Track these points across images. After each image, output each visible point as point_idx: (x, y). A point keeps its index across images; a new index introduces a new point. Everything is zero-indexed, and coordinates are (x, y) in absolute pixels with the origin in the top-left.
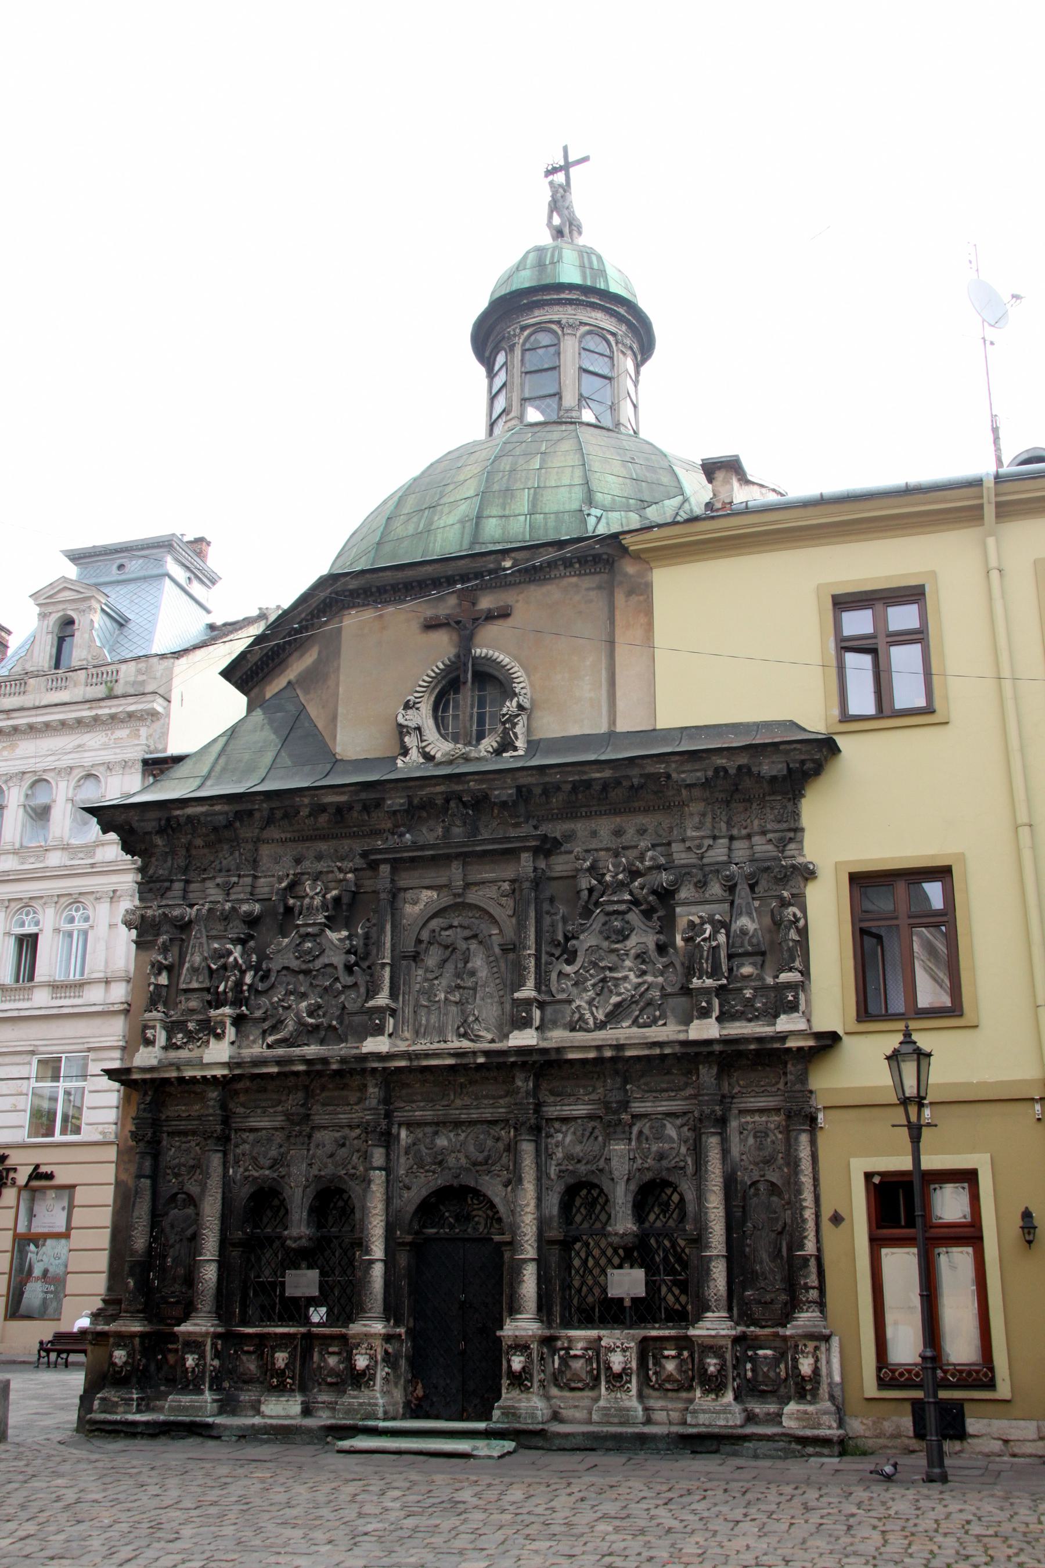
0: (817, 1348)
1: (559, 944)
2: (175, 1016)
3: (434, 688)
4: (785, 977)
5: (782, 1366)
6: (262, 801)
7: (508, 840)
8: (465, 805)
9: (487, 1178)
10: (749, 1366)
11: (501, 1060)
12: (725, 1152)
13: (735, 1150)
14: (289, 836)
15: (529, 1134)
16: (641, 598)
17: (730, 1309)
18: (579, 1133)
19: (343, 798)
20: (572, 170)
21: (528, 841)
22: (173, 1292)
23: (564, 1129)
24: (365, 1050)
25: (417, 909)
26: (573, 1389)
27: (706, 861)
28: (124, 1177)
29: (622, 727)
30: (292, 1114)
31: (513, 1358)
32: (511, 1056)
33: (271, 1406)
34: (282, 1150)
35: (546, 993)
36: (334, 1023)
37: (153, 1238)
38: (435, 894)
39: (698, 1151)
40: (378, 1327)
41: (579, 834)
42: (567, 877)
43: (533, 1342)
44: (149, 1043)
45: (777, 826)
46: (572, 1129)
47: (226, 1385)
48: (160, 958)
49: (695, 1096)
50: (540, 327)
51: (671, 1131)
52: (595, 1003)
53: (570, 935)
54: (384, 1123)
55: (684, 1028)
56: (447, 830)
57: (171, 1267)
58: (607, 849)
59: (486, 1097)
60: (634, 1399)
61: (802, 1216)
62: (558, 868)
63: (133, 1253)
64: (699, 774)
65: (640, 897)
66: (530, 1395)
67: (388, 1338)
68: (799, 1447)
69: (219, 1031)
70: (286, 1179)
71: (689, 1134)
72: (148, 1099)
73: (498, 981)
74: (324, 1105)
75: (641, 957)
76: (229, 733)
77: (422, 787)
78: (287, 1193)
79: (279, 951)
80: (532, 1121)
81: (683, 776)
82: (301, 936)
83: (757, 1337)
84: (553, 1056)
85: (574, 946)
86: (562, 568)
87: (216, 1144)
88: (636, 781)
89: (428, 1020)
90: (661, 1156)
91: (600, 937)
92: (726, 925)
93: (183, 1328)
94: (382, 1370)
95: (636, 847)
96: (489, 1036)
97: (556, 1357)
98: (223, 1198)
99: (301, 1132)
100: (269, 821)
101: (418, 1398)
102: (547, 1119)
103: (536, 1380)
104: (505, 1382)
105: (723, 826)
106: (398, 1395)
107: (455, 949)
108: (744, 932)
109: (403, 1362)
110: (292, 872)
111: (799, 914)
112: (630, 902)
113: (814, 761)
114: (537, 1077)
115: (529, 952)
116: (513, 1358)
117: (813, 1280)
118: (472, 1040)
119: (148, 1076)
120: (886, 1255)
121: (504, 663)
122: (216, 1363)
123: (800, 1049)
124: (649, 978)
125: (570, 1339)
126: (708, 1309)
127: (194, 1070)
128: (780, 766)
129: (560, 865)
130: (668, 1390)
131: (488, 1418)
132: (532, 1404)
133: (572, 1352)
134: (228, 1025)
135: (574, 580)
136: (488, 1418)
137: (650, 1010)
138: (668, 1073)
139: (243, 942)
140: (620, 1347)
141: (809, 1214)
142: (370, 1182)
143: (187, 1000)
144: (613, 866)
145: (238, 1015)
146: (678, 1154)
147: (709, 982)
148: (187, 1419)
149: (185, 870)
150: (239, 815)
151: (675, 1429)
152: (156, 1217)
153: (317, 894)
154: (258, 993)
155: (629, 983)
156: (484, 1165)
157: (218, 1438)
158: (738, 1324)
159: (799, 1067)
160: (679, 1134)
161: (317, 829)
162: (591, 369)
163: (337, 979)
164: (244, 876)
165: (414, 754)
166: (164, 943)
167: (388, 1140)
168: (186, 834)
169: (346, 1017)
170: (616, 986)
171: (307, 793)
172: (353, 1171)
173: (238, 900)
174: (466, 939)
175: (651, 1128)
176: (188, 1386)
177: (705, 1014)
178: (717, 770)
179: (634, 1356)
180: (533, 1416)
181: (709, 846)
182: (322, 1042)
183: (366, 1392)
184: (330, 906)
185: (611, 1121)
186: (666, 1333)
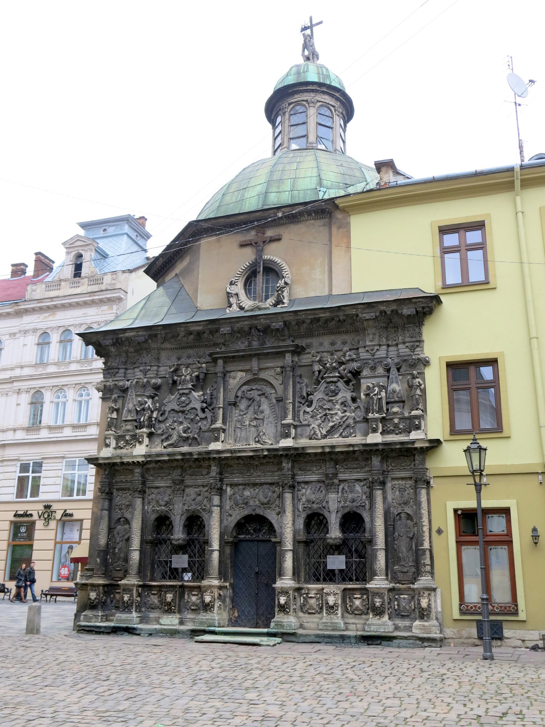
1: (304, 398)
2: (120, 433)
3: (244, 275)
4: (414, 413)
5: (412, 603)
6: (162, 330)
7: (280, 347)
8: (259, 331)
10: (396, 603)
11: (275, 453)
12: (385, 498)
13: (390, 498)
14: (174, 346)
16: (345, 230)
17: (387, 575)
18: (313, 489)
19: (200, 328)
20: (314, 28)
21: (289, 347)
23: (306, 487)
24: (210, 449)
25: (235, 381)
26: (310, 613)
27: (375, 357)
28: (96, 510)
29: (334, 293)
30: (176, 480)
31: (281, 598)
32: (280, 451)
33: (164, 620)
34: (170, 497)
35: (297, 421)
36: (196, 436)
37: (109, 539)
38: (244, 374)
39: (371, 497)
40: (216, 582)
41: (314, 344)
42: (308, 365)
44: (107, 446)
47: (143, 609)
48: (113, 405)
49: (370, 471)
50: (298, 103)
51: (358, 488)
52: (321, 426)
53: (309, 393)
54: (219, 484)
55: (365, 438)
56: (250, 344)
57: (118, 553)
58: (328, 352)
59: (269, 471)
60: (340, 618)
61: (422, 530)
62: (304, 361)
63: (99, 546)
64: (372, 314)
65: (344, 374)
67: (220, 588)
68: (420, 643)
69: (140, 440)
72: (107, 472)
73: (274, 416)
74: (191, 475)
75: (343, 404)
76: (147, 298)
77: (238, 322)
78: (173, 518)
79: (170, 402)
80: (291, 483)
81: (364, 315)
82: (180, 395)
83: (399, 589)
84: (300, 451)
85: (311, 398)
86: (306, 216)
87: (139, 494)
88: (341, 318)
89: (241, 434)
90: (353, 501)
91: (324, 394)
92: (385, 388)
93: (123, 582)
95: (341, 350)
96: (270, 442)
97: (302, 598)
98: (142, 520)
100: (165, 340)
101: (235, 617)
102: (298, 482)
103: (292, 609)
104: (277, 609)
105: (384, 340)
106: (225, 616)
107: (254, 400)
108: (394, 391)
109: (228, 600)
110: (176, 363)
111: (421, 382)
112: (339, 377)
113: (428, 307)
114: (293, 462)
116: (281, 598)
117: (428, 561)
118: (262, 444)
119: (107, 461)
120: (464, 549)
121: (278, 262)
122: (139, 599)
123: (422, 448)
124: (348, 414)
125: (308, 589)
128: (412, 310)
129: (305, 359)
130: (356, 614)
131: (267, 626)
132: (290, 620)
133: (309, 595)
134: (145, 437)
135: (312, 221)
136: (267, 626)
137: (348, 429)
138: (357, 459)
139: (153, 398)
140: (333, 592)
141: (426, 529)
142: (212, 512)
144: (331, 359)
145: (150, 432)
146: (361, 500)
147: (377, 415)
148: (125, 625)
149: (125, 363)
150: (150, 337)
151: (359, 633)
152: (110, 530)
156: (267, 505)
157: (139, 635)
158: (391, 582)
160: (362, 490)
161: (188, 343)
162: (323, 123)
163: (197, 415)
165: (235, 307)
166: (115, 398)
167: (221, 492)
168: (126, 346)
169: (201, 433)
170: (332, 418)
171: (183, 325)
174: (259, 395)
175: (349, 486)
176: (125, 610)
177: (375, 431)
178: (381, 312)
179: (340, 598)
180: (290, 626)
183: (210, 613)
185: (329, 483)
186: (355, 586)
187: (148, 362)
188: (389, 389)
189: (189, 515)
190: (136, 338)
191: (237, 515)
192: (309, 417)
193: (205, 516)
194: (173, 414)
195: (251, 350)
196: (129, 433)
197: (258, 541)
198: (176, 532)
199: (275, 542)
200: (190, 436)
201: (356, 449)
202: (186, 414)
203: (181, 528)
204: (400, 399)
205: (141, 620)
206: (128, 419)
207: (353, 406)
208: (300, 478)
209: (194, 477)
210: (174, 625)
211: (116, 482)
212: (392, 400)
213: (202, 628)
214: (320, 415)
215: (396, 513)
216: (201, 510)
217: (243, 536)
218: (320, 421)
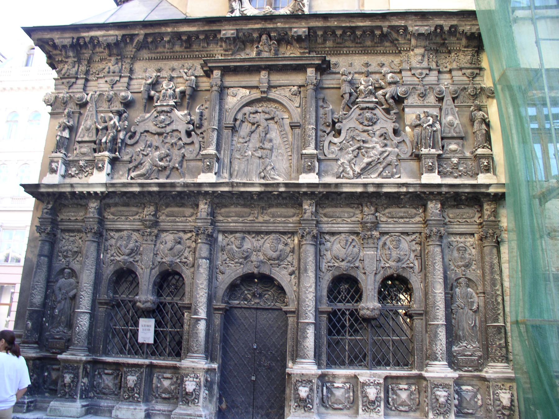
9: (277, 269)
11: (296, 190)
15: (312, 240)
21: (314, 60)
22: (58, 332)
25: (235, 100)
28: (31, 256)
30: (146, 221)
31: (300, 388)
33: (124, 412)
34: (137, 244)
36: (177, 165)
37: (46, 297)
38: (247, 91)
39: (422, 256)
52: (354, 161)
53: (336, 121)
57: (58, 315)
59: (280, 216)
64: (426, 28)
66: (311, 414)
67: (209, 371)
69: (100, 165)
70: (139, 263)
72: (50, 206)
73: (287, 146)
74: (167, 216)
81: (417, 28)
82: (158, 112)
84: (333, 190)
85: (339, 126)
89: (239, 168)
90: (399, 260)
93: (63, 356)
94: (204, 392)
98: (96, 273)
99: (151, 233)
107: (258, 126)
109: (216, 387)
112: (377, 103)
115: (312, 126)
116: (300, 388)
119: (51, 190)
124: (389, 149)
125: (334, 376)
127: (83, 187)
133: (336, 385)
134: (106, 162)
139: (119, 114)
143: (81, 147)
144: (365, 81)
145: (113, 158)
147: (433, 151)
152: (49, 283)
155: (376, 151)
159: (492, 206)
163: (180, 139)
167: (211, 240)
169: (185, 163)
172: (186, 260)
173: (118, 90)
174: (267, 120)
176: (66, 394)
177: (431, 170)
179: (382, 389)
181: (427, 74)
183: (192, 406)
184: (178, 97)
188: (444, 121)
191: (231, 272)
192: (337, 149)
193: (186, 273)
195: (262, 59)
197: (257, 309)
199: (286, 312)
201: (411, 190)
202: (166, 137)
206: (84, 139)
207: (397, 139)
208: (326, 228)
209: (172, 218)
211: (62, 220)
212: (450, 135)
214: (352, 148)
215: (455, 279)
218: (351, 156)
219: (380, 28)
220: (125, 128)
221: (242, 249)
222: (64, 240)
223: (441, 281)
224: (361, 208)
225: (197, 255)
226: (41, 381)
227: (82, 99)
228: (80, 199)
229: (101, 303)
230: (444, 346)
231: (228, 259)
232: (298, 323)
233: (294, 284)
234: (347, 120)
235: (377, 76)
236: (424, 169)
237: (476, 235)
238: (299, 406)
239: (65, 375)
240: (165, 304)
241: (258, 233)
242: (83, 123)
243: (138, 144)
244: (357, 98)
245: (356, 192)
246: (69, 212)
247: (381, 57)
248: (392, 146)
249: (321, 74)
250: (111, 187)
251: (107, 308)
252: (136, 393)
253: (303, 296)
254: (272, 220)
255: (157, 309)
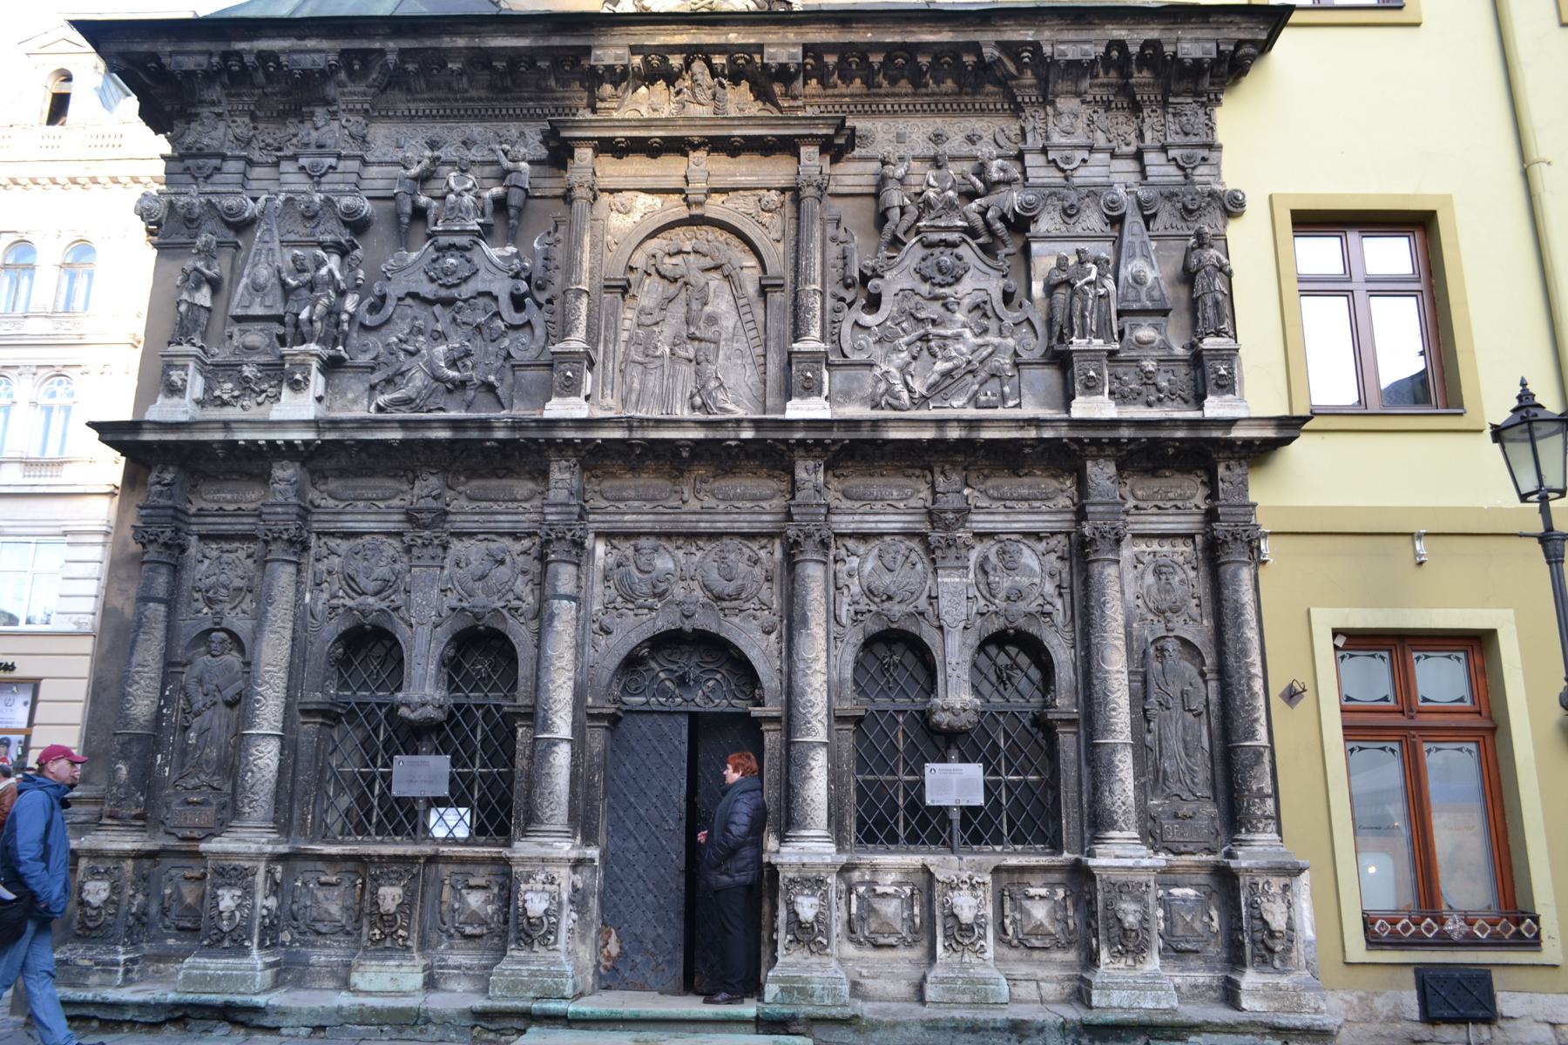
0: (1286, 888)
2: (221, 354)
9: (737, 620)
11: (781, 435)
23: (862, 549)
24: (547, 415)
26: (877, 946)
27: (1077, 181)
28: (117, 602)
30: (420, 511)
31: (799, 899)
32: (797, 429)
33: (370, 976)
36: (492, 378)
38: (656, 201)
40: (566, 848)
41: (879, 136)
43: (829, 873)
44: (174, 390)
45: (1179, 139)
46: (876, 551)
47: (285, 937)
48: (200, 264)
51: (1028, 558)
53: (869, 273)
57: (196, 747)
58: (923, 159)
59: (742, 498)
60: (991, 963)
61: (1250, 688)
62: (849, 180)
64: (1086, 47)
66: (825, 959)
67: (578, 864)
69: (298, 377)
71: (1058, 565)
73: (753, 334)
74: (471, 499)
78: (402, 633)
79: (403, 269)
81: (1062, 47)
82: (438, 249)
84: (865, 434)
87: (285, 551)
88: (989, 52)
89: (642, 383)
90: (1017, 595)
91: (917, 277)
98: (293, 640)
101: (609, 957)
106: (586, 954)
108: (1138, 280)
109: (594, 903)
112: (965, 230)
116: (799, 899)
120: (1429, 751)
122: (272, 902)
123: (1248, 443)
124: (993, 339)
125: (874, 869)
126: (1113, 825)
129: (853, 175)
130: (1033, 948)
132: (831, 974)
133: (880, 890)
137: (994, 384)
139: (343, 251)
141: (1258, 685)
142: (552, 616)
143: (244, 332)
144: (936, 179)
145: (330, 357)
147: (1098, 343)
152: (171, 666)
153: (467, 190)
154: (365, 328)
157: (275, 1030)
163: (498, 314)
164: (348, 157)
166: (207, 244)
170: (944, 347)
172: (518, 603)
173: (334, 191)
177: (1091, 388)
179: (989, 896)
181: (1084, 161)
182: (468, 407)
183: (541, 951)
185: (935, 539)
186: (1032, 861)
187: (329, 142)
188: (1123, 273)
189: (461, 625)
190: (295, 57)
191: (632, 630)
192: (871, 340)
194: (414, 308)
195: (691, 121)
196: (256, 358)
198: (416, 681)
199: (758, 722)
200: (471, 379)
201: (1048, 434)
203: (432, 668)
204: (1158, 306)
205: (277, 975)
206: (251, 312)
207: (1010, 317)
209: (484, 504)
210: (405, 994)
211: (201, 513)
212: (1135, 306)
213: (520, 1004)
214: (906, 339)
216: (505, 612)
217: (643, 699)
218: (905, 356)
219: (975, 48)
220: (358, 286)
221: (654, 574)
222: (207, 562)
223: (1120, 644)
224: (929, 478)
225: (548, 591)
226: (154, 909)
227: (240, 212)
228: (250, 461)
229: (305, 712)
230: (1131, 794)
231: (620, 599)
232: (789, 744)
233: (776, 653)
234: (895, 272)
235: (967, 167)
236: (1077, 386)
237: (1198, 539)
238: (798, 941)
239: (220, 892)
240: (469, 708)
241: (692, 536)
242: (246, 272)
243: (391, 326)
244: (918, 219)
245: (919, 441)
246: (218, 491)
247: (973, 120)
248: (1001, 333)
249: (835, 160)
250: (330, 430)
251: (322, 724)
252: (402, 927)
253: (800, 681)
254: (722, 506)
255: (448, 721)
